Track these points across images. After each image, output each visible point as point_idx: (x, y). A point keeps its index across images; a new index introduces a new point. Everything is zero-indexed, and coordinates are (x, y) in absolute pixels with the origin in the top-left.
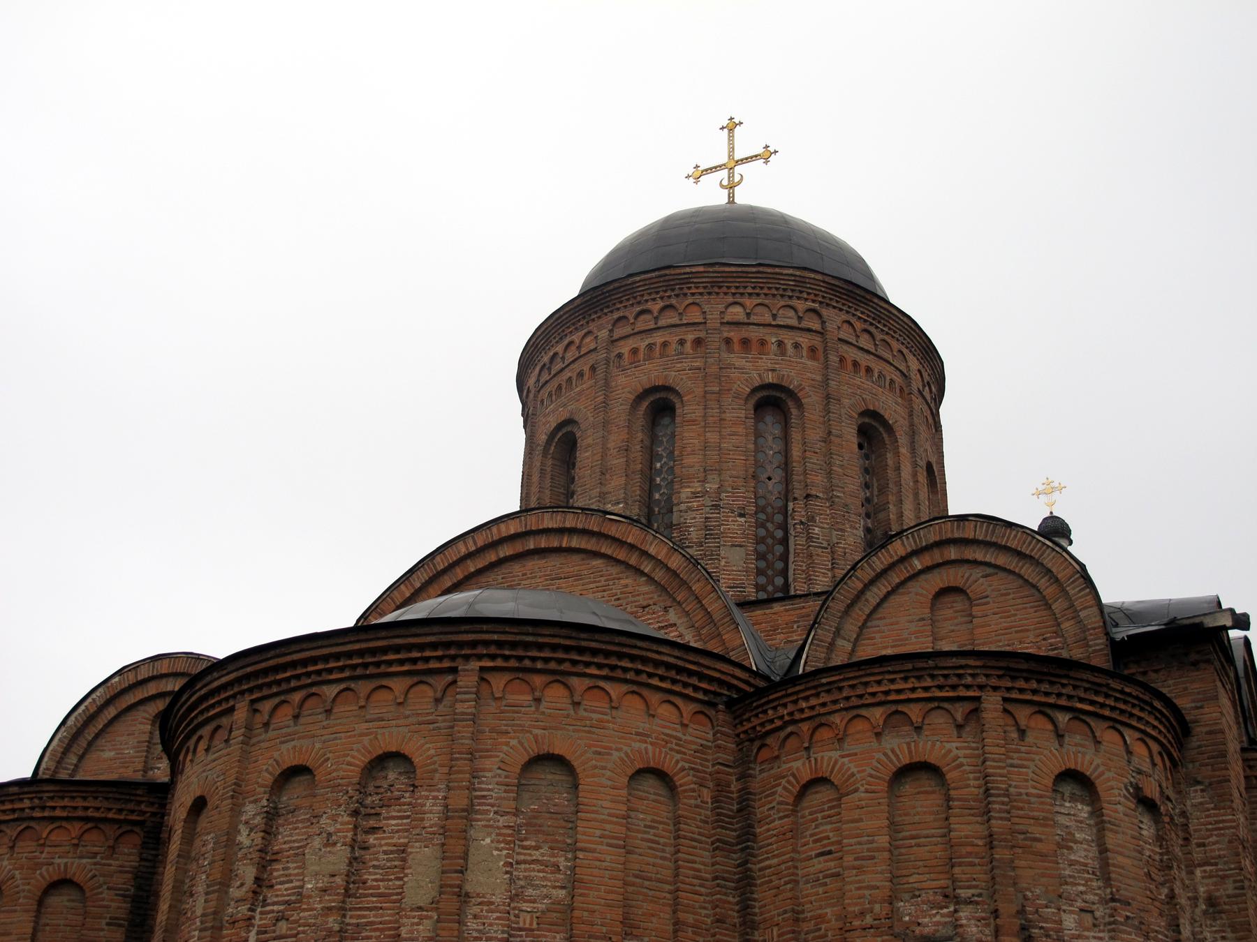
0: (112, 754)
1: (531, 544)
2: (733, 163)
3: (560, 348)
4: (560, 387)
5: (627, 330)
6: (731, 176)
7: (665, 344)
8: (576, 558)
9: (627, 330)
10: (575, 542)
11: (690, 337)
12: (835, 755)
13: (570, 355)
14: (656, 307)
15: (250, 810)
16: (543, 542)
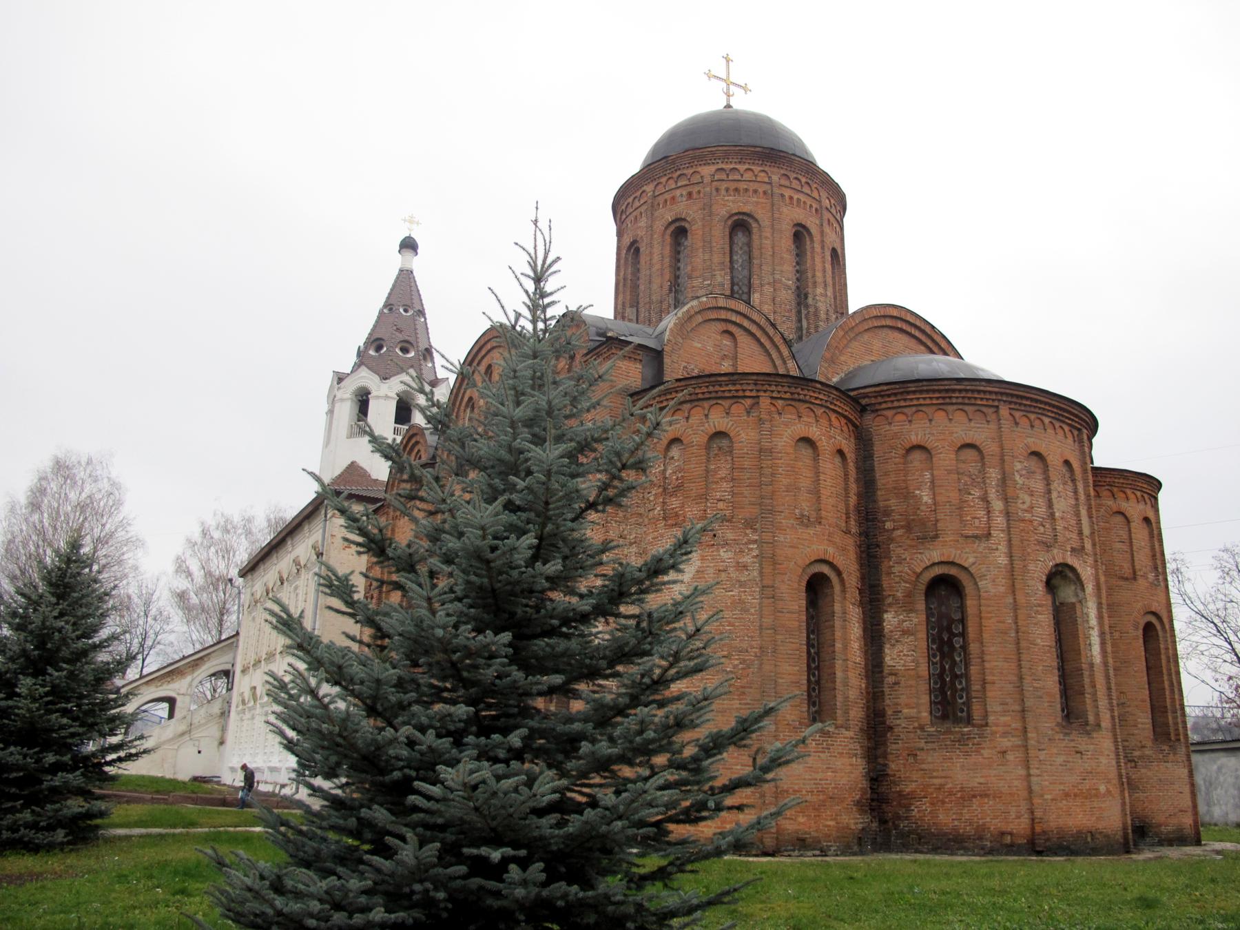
0: (700, 345)
1: (899, 324)
2: (727, 81)
3: (742, 167)
4: (736, 190)
5: (787, 183)
6: (728, 89)
7: (804, 202)
8: (914, 341)
9: (787, 183)
10: (913, 331)
11: (815, 206)
12: (1126, 505)
13: (748, 176)
14: (803, 180)
15: (1018, 466)
16: (905, 327)
